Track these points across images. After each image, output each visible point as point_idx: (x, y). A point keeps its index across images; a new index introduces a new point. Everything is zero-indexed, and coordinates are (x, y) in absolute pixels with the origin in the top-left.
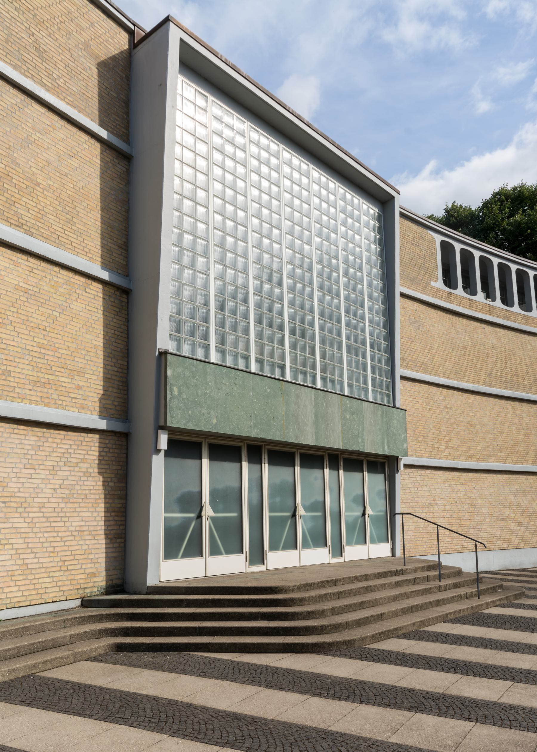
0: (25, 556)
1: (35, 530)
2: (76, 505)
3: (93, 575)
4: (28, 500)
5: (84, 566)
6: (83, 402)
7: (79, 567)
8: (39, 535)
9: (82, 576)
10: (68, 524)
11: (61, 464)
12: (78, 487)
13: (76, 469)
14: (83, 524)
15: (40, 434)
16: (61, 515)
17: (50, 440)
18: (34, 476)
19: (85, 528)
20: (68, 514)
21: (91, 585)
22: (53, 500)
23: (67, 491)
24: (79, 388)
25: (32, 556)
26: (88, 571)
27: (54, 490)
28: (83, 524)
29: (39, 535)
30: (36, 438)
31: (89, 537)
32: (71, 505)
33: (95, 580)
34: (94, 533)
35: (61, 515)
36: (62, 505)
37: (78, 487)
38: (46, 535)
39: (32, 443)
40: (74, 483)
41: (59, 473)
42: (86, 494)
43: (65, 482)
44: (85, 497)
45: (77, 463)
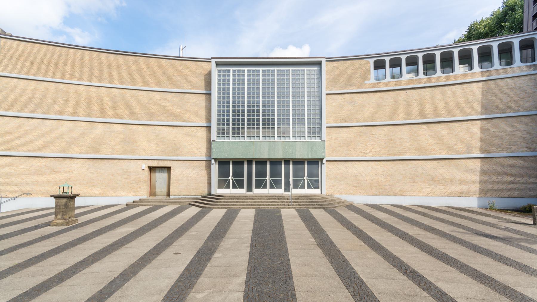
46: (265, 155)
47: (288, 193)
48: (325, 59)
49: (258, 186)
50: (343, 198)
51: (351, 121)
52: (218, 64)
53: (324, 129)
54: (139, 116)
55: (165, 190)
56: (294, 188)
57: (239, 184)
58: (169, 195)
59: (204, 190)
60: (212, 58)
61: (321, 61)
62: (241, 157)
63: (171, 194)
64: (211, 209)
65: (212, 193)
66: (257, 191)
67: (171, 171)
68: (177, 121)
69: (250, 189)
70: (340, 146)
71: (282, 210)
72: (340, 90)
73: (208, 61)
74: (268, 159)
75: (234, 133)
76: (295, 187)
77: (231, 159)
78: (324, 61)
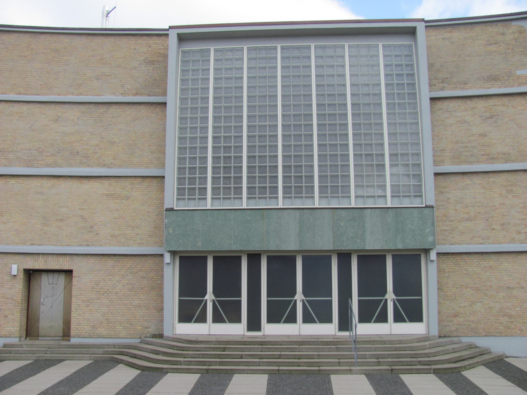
0: (108, 315)
1: (114, 304)
2: (136, 293)
3: (147, 328)
4: (110, 290)
5: (141, 323)
6: (140, 241)
7: (138, 323)
8: (116, 306)
9: (141, 328)
10: (132, 302)
11: (127, 273)
12: (137, 284)
13: (136, 275)
14: (140, 302)
15: (116, 260)
16: (128, 297)
17: (121, 262)
18: (113, 279)
19: (142, 304)
20: (132, 297)
21: (146, 332)
22: (123, 290)
23: (131, 286)
24: (137, 234)
25: (112, 315)
26: (144, 325)
27: (124, 285)
28: (140, 302)
29: (116, 306)
30: (113, 262)
31: (145, 309)
32: (133, 293)
33: (149, 330)
34: (147, 307)
35: (128, 297)
36: (129, 293)
37: (137, 284)
38: (119, 306)
39: (111, 264)
40: (135, 282)
41: (126, 277)
42: (142, 288)
43: (130, 282)
44: (142, 288)
45: (137, 273)
46: (290, 244)
47: (346, 333)
48: (424, 24)
49: (273, 319)
50: (482, 342)
51: (492, 159)
52: (182, 38)
53: (429, 181)
54: (11, 156)
55: (59, 325)
56: (361, 320)
57: (227, 312)
58: (66, 334)
59: (146, 324)
60: (171, 27)
61: (415, 27)
62: (234, 248)
63: (72, 333)
64: (163, 372)
65: (167, 333)
66: (271, 330)
67: (75, 280)
68: (89, 166)
69: (254, 324)
70: (469, 219)
71: (331, 376)
72: (463, 89)
73: (161, 34)
74: (299, 252)
75: (215, 190)
76: (365, 318)
77: (210, 252)
78: (421, 29)
